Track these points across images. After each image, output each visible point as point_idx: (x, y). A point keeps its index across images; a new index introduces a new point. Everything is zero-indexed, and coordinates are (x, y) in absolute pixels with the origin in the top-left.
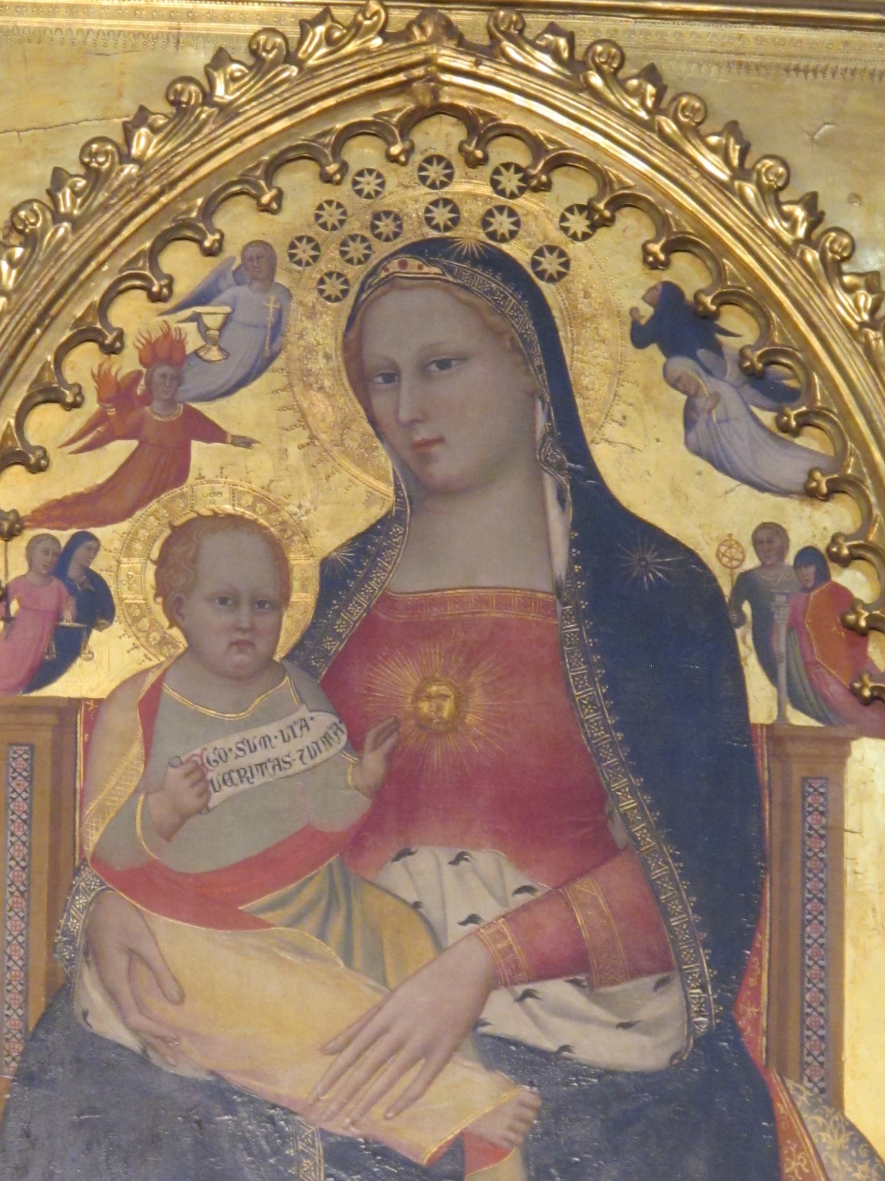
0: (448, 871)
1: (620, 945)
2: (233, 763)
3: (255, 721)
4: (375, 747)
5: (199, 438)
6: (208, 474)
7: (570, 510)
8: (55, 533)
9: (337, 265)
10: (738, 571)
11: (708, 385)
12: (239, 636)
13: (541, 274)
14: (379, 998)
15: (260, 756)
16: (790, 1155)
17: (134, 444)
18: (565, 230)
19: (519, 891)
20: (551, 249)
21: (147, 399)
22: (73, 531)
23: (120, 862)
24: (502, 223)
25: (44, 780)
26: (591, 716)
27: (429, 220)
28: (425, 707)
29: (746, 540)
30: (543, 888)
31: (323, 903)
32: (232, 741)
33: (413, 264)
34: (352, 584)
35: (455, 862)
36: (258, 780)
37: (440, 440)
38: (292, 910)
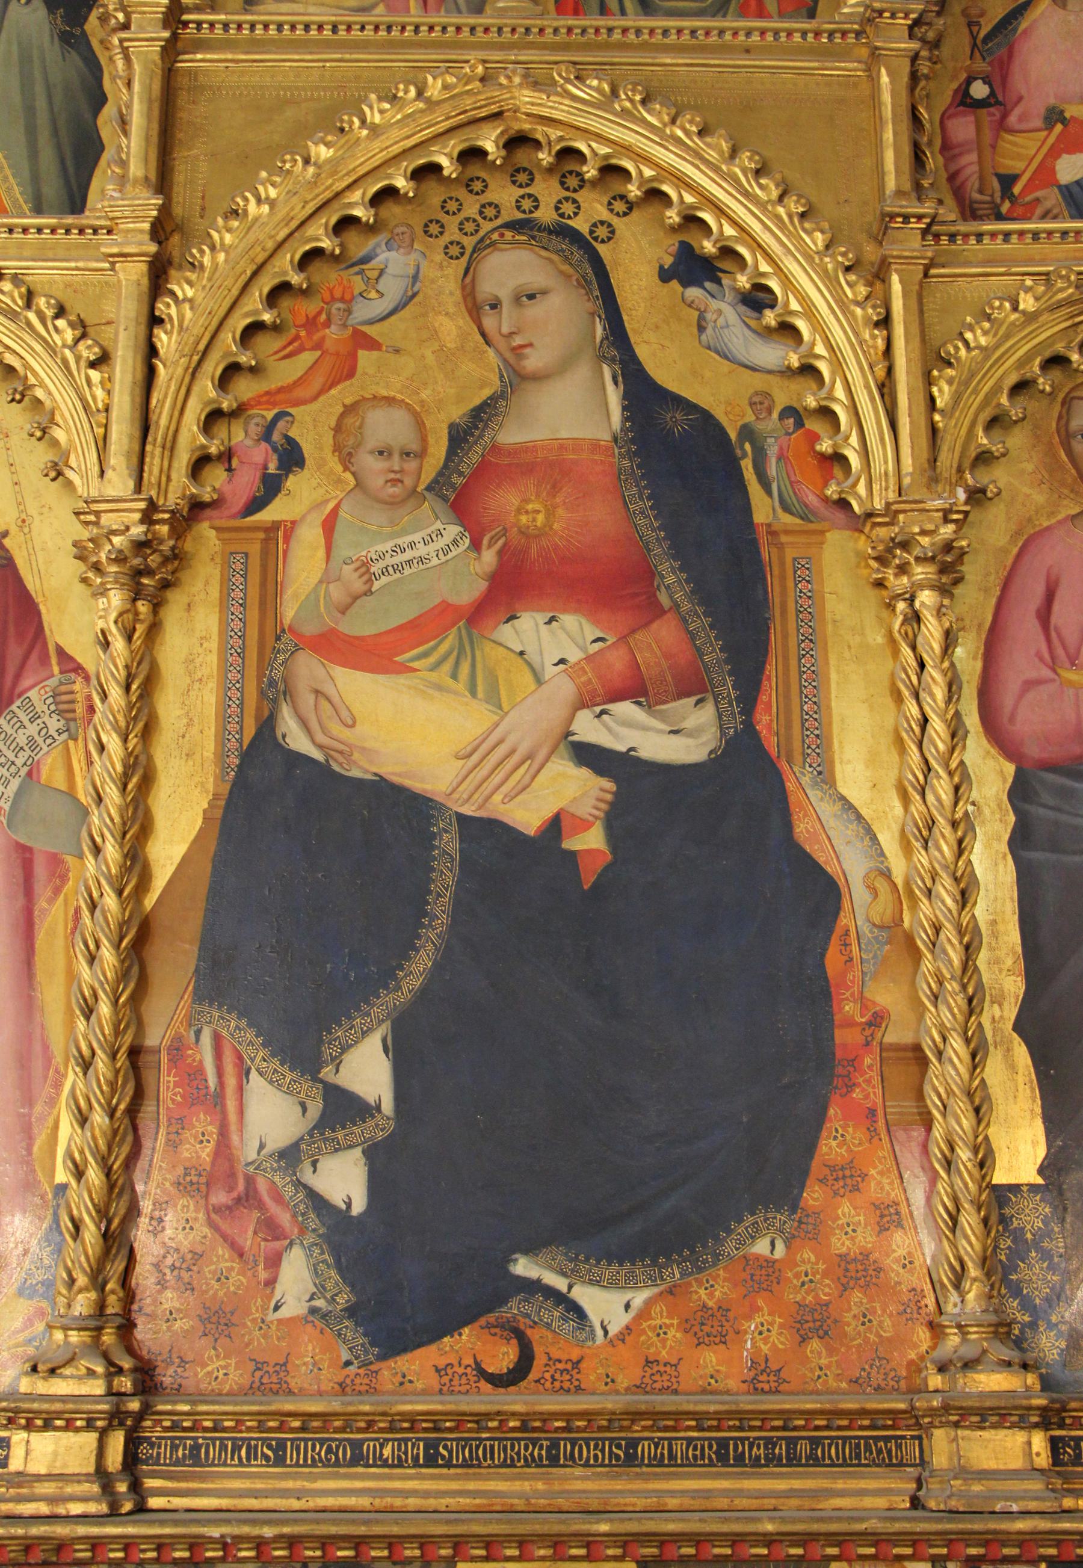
0: (544, 629)
1: (669, 678)
2: (389, 561)
3: (404, 532)
4: (489, 547)
5: (363, 348)
6: (371, 371)
7: (622, 387)
8: (264, 413)
9: (457, 236)
10: (740, 423)
11: (714, 304)
12: (392, 476)
13: (596, 239)
14: (496, 718)
15: (409, 555)
16: (799, 819)
17: (318, 353)
18: (612, 211)
19: (594, 641)
20: (602, 223)
21: (328, 324)
22: (276, 411)
23: (309, 629)
24: (568, 208)
25: (255, 577)
26: (641, 521)
27: (518, 208)
28: (524, 519)
29: (745, 403)
30: (611, 640)
31: (455, 653)
32: (388, 546)
33: (509, 234)
34: (471, 440)
35: (549, 622)
36: (407, 571)
37: (531, 345)
38: (432, 660)
